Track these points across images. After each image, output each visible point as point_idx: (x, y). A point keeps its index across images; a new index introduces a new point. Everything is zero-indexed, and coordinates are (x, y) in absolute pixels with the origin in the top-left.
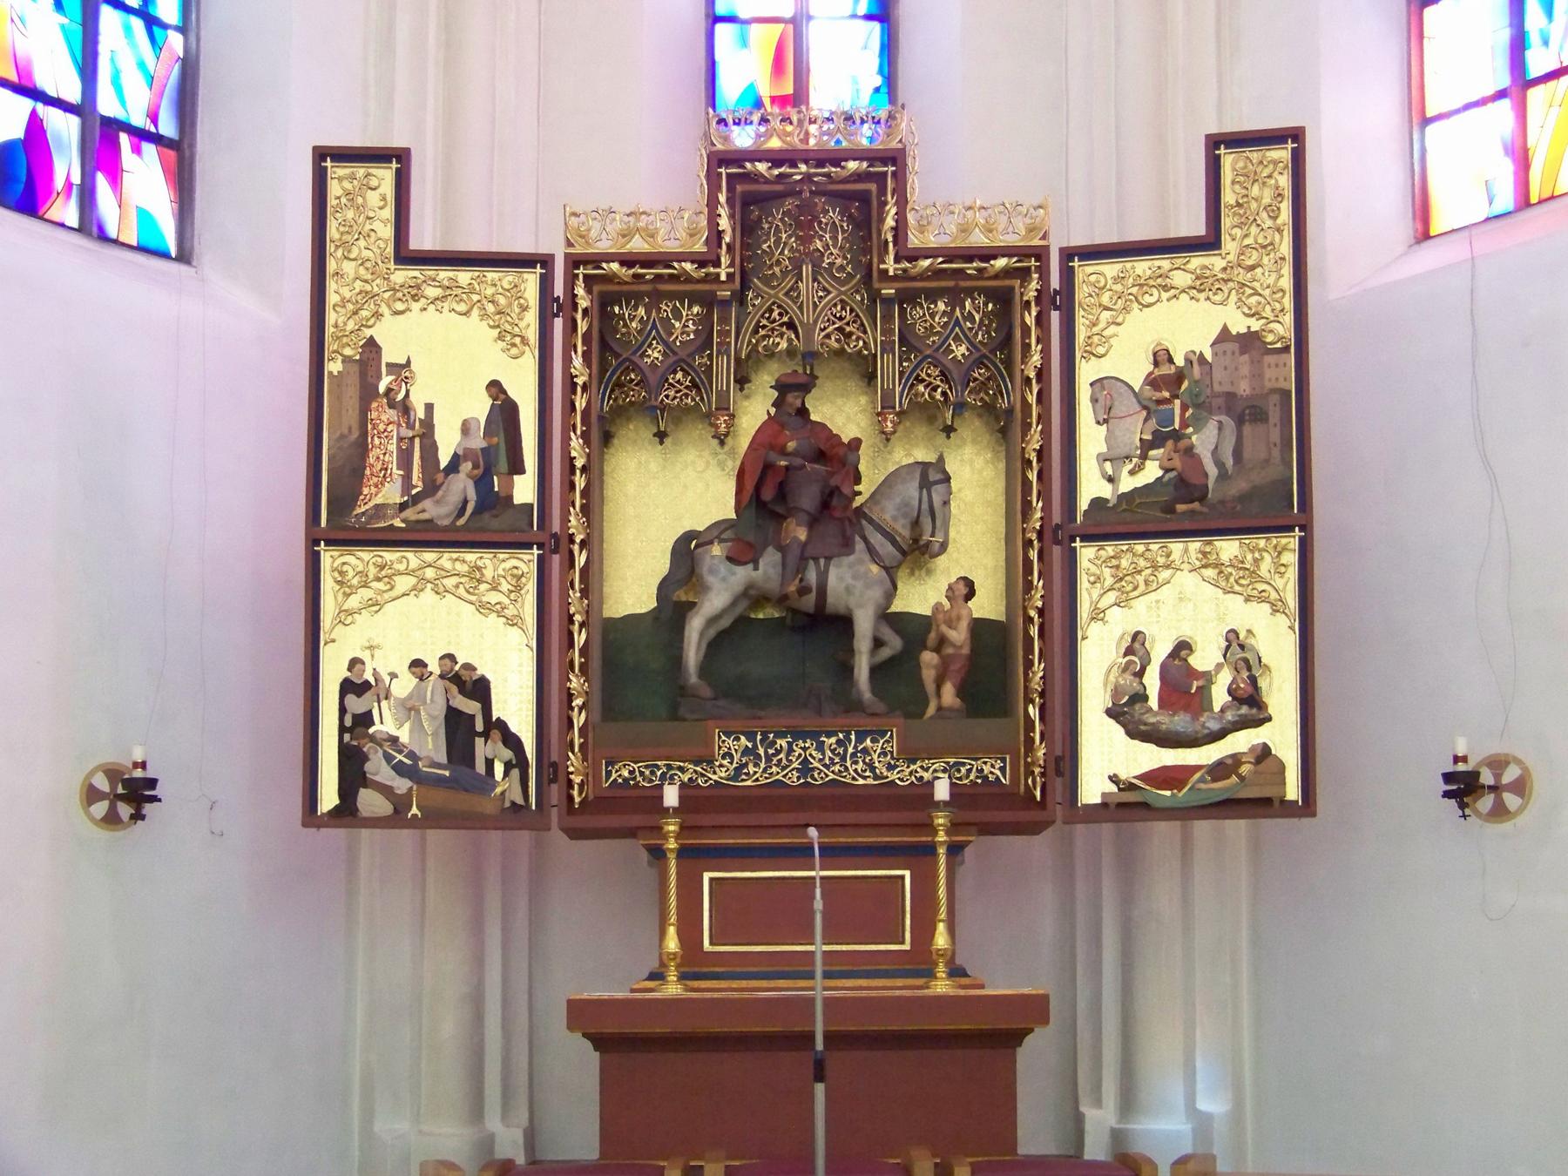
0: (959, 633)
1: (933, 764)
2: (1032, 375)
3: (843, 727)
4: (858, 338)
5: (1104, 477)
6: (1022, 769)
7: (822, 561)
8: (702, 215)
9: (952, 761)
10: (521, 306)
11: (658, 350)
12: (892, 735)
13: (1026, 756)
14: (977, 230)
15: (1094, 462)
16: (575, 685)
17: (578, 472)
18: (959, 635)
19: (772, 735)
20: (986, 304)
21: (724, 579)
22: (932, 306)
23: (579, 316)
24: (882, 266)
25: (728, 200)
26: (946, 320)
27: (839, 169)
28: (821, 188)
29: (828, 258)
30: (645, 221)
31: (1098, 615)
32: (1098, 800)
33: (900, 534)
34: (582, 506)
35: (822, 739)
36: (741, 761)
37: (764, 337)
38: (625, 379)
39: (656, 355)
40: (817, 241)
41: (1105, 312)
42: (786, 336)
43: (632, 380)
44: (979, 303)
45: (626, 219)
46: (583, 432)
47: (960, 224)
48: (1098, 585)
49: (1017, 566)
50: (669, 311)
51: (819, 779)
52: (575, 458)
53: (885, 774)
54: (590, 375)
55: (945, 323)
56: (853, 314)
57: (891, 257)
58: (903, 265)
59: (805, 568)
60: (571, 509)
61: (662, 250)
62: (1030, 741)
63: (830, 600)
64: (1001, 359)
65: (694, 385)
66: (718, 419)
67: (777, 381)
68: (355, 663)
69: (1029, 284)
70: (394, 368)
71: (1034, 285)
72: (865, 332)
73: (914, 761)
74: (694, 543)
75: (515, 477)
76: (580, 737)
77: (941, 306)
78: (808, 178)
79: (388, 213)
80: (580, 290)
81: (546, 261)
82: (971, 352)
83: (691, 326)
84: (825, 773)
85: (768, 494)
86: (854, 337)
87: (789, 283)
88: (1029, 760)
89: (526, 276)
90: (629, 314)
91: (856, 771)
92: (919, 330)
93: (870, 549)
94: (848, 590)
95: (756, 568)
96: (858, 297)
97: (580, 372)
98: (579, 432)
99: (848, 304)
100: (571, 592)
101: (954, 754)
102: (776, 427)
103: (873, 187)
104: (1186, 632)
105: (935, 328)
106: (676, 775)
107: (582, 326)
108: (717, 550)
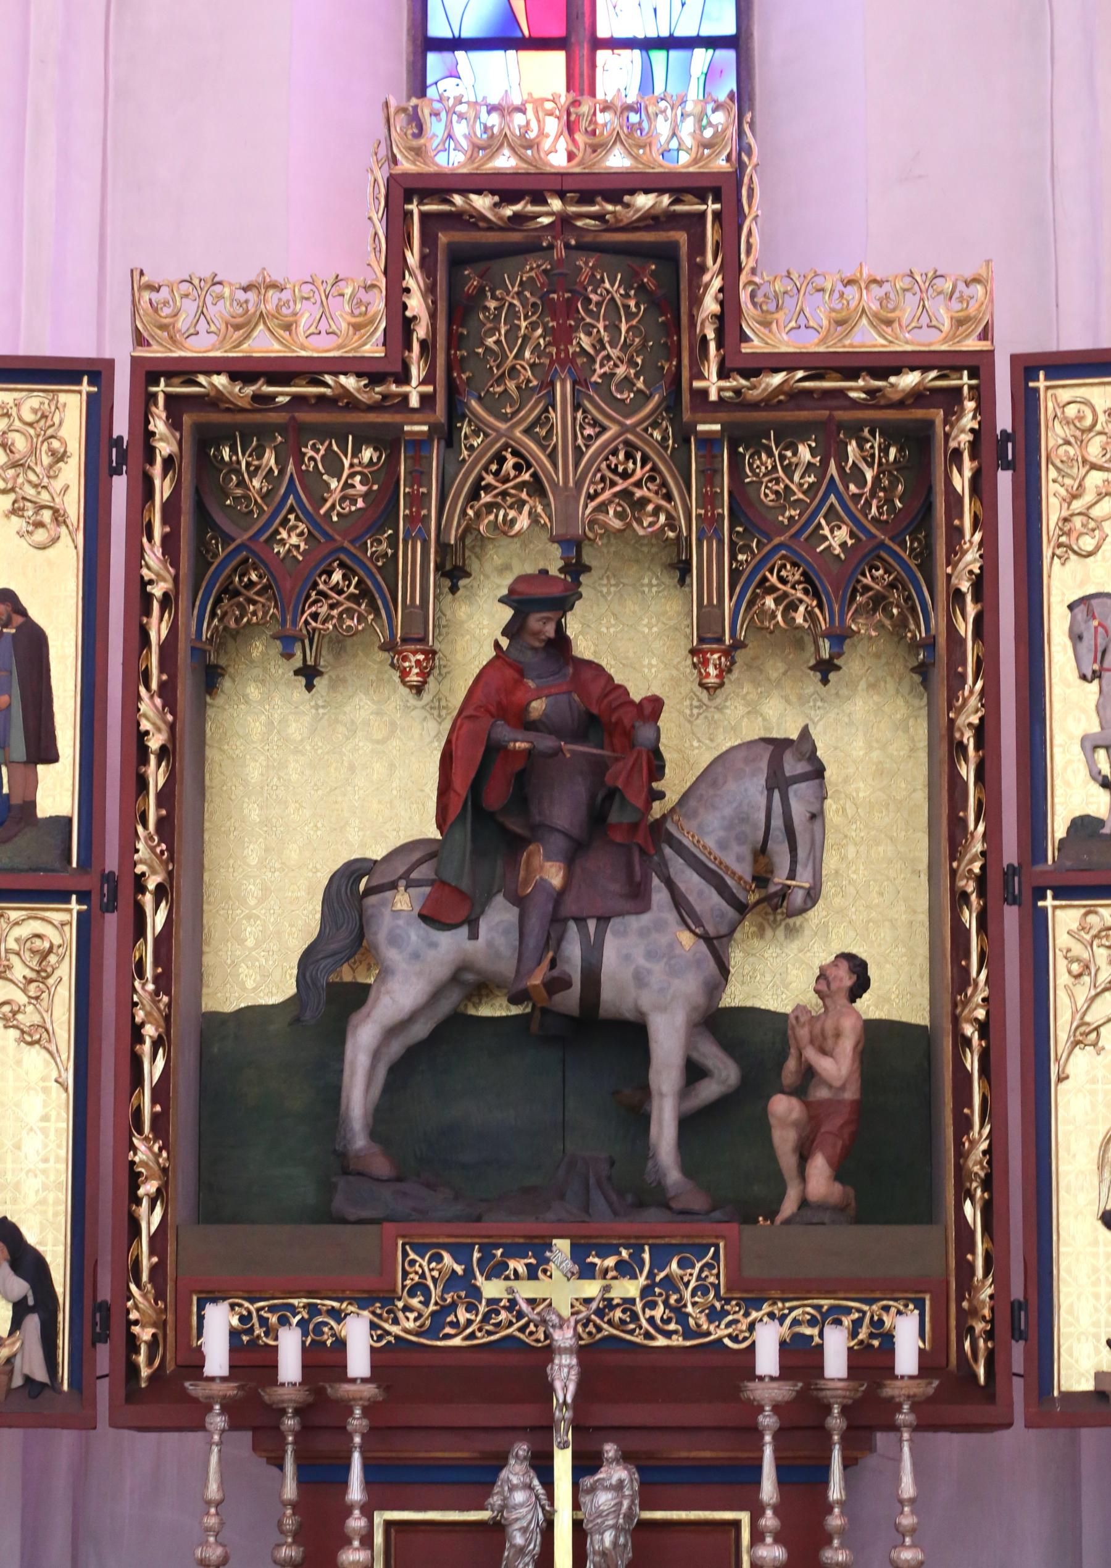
0: (837, 1062)
1: (792, 1309)
2: (965, 586)
3: (629, 1237)
4: (656, 512)
5: (1094, 779)
6: (953, 1322)
7: (592, 924)
8: (376, 291)
9: (826, 1303)
10: (53, 453)
11: (298, 531)
12: (717, 1252)
13: (960, 1299)
14: (864, 321)
15: (1077, 748)
16: (144, 1157)
17: (153, 759)
19: (499, 1252)
20: (885, 451)
21: (416, 956)
22: (789, 454)
23: (157, 470)
24: (697, 384)
25: (423, 259)
26: (812, 479)
27: (619, 208)
28: (588, 238)
29: (602, 366)
30: (275, 301)
32: (1088, 1385)
33: (734, 873)
34: (160, 821)
35: (591, 1259)
36: (445, 1300)
37: (490, 507)
38: (241, 581)
39: (294, 540)
40: (582, 336)
41: (1094, 473)
42: (526, 508)
43: (251, 584)
44: (872, 447)
45: (241, 296)
46: (162, 685)
47: (833, 310)
48: (1086, 979)
49: (943, 942)
50: (318, 458)
51: (585, 1336)
52: (147, 733)
53: (705, 1327)
54: (176, 579)
55: (811, 485)
56: (648, 467)
57: (712, 369)
58: (735, 383)
59: (560, 940)
60: (140, 829)
61: (303, 354)
62: (966, 1270)
63: (607, 993)
64: (912, 549)
65: (364, 593)
66: (405, 659)
67: (512, 591)
69: (959, 419)
71: (968, 421)
72: (669, 497)
73: (757, 1304)
74: (364, 881)
75: (41, 768)
76: (151, 1253)
77: (805, 453)
78: (564, 221)
80: (159, 425)
82: (858, 539)
83: (359, 487)
84: (596, 1326)
85: (496, 797)
86: (650, 508)
87: (531, 411)
88: (965, 1304)
89: (63, 398)
90: (248, 464)
91: (651, 1320)
92: (766, 495)
93: (679, 901)
94: (640, 979)
95: (474, 935)
96: (657, 435)
97: (158, 575)
98: (154, 685)
99: (637, 449)
100: (137, 984)
101: (828, 1293)
102: (510, 673)
103: (682, 237)
105: (794, 494)
106: (326, 1324)
107: (163, 489)
108: (403, 901)
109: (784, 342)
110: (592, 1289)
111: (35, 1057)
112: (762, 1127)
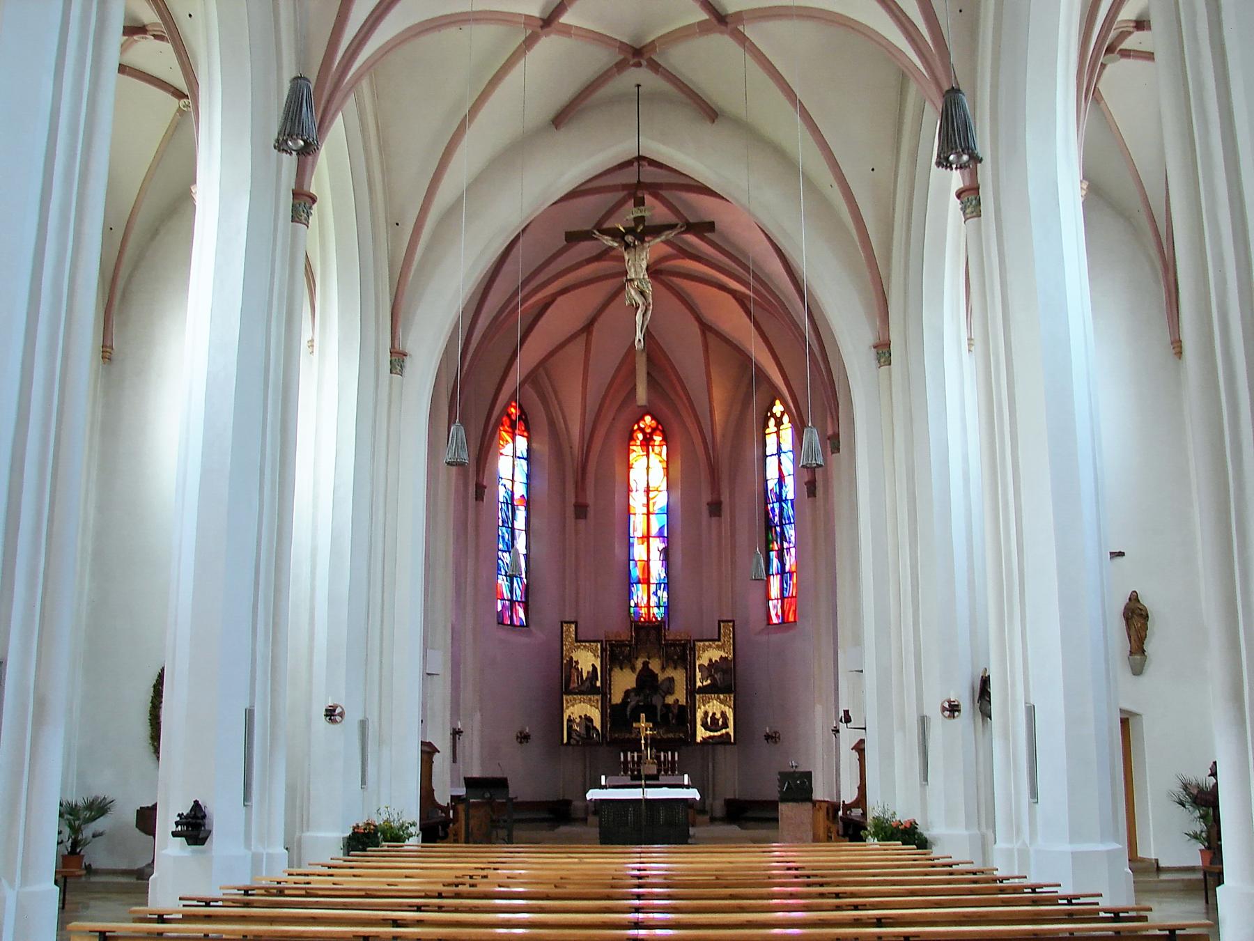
18: (676, 711)
68: (570, 716)
70: (575, 662)
79: (574, 633)
81: (602, 641)
104: (715, 711)
111: (597, 710)
112: (668, 716)
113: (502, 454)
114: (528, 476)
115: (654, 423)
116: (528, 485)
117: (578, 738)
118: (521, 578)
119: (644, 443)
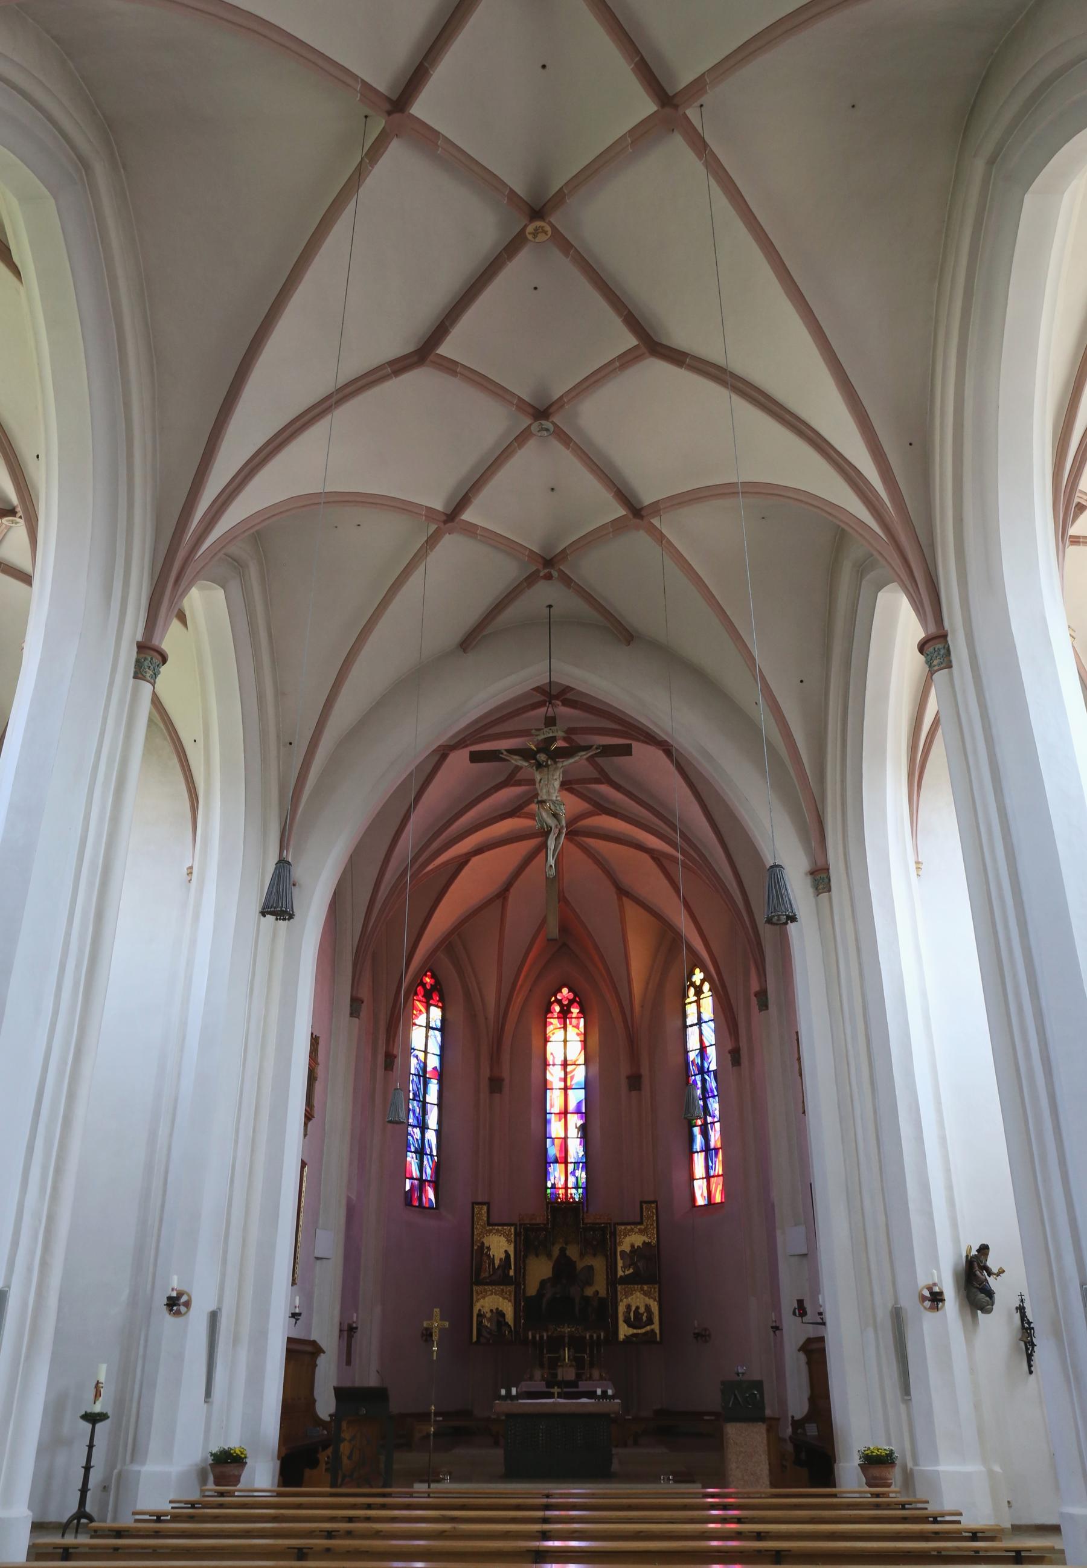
31: (622, 1300)
68: (480, 1310)
79: (486, 1215)
80: (522, 1230)
104: (638, 1304)
109: (590, 1221)
110: (569, 1330)
111: (510, 1304)
113: (415, 1024)
114: (442, 1047)
115: (571, 996)
116: (442, 1056)
117: (488, 1336)
118: (432, 1155)
119: (561, 1015)
